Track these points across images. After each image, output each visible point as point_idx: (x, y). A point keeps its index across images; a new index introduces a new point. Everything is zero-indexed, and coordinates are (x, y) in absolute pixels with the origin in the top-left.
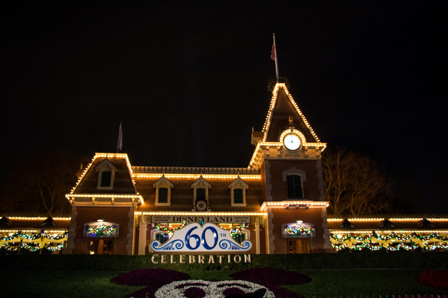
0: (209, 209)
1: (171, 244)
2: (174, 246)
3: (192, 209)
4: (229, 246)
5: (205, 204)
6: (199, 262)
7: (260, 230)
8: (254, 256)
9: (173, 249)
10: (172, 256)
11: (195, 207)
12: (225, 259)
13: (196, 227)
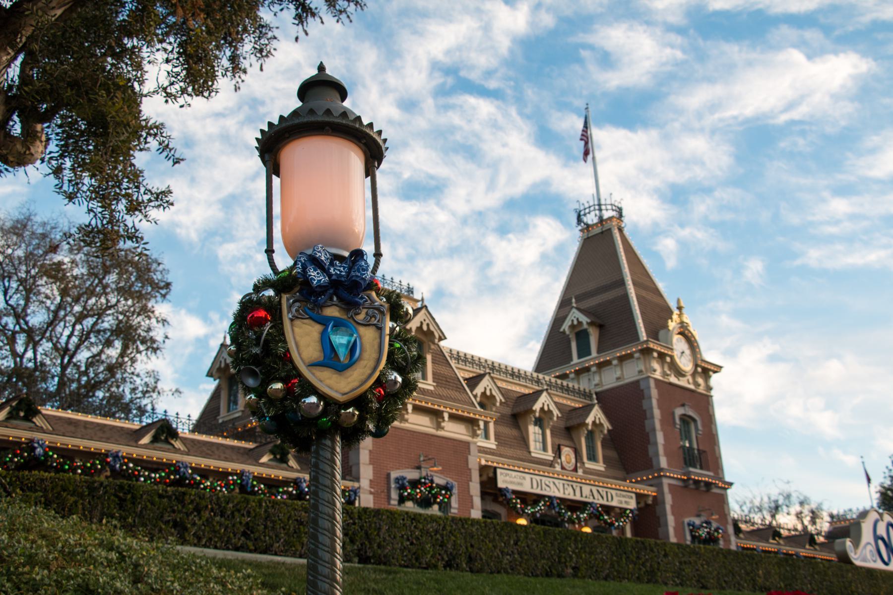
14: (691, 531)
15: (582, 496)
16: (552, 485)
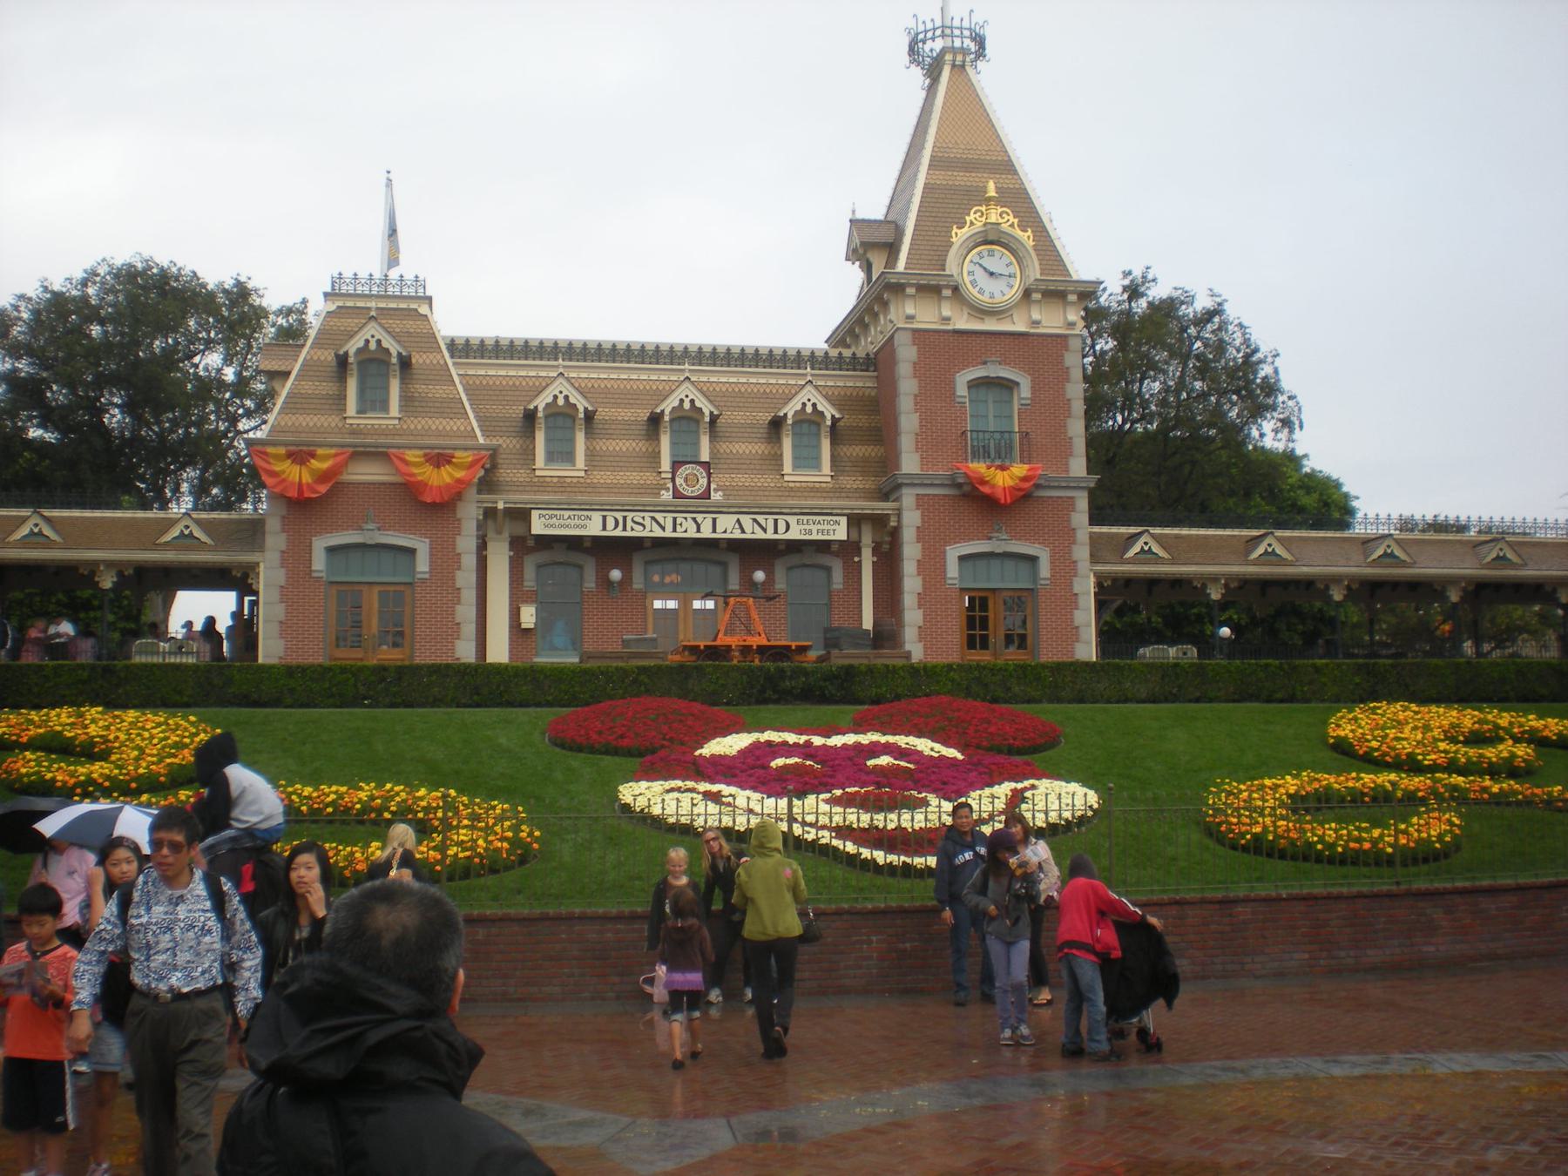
3: (663, 492)
5: (704, 474)
11: (670, 485)
15: (714, 531)
16: (647, 522)
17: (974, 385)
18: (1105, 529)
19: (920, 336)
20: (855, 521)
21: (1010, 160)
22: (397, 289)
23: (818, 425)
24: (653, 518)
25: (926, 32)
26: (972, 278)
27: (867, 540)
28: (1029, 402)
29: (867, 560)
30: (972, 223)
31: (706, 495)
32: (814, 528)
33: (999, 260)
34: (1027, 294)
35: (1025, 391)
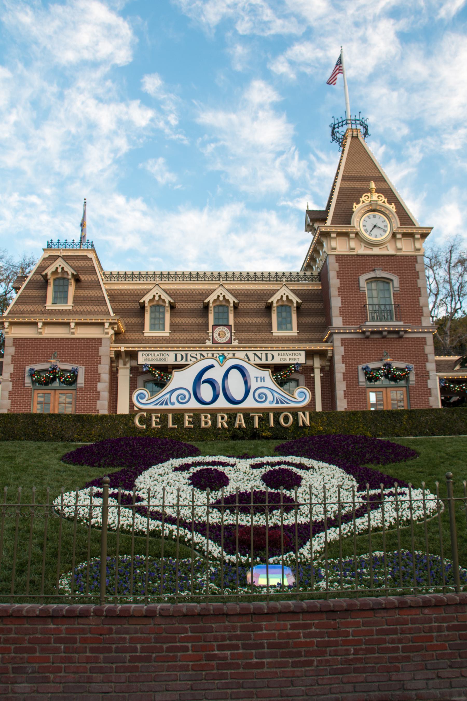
0: (235, 340)
1: (168, 396)
2: (174, 399)
3: (207, 341)
4: (270, 398)
5: (229, 331)
6: (220, 425)
7: (322, 375)
8: (314, 416)
9: (173, 404)
10: (170, 416)
11: (211, 338)
12: (264, 419)
13: (212, 366)
14: (366, 374)
17: (370, 281)
18: (442, 358)
19: (339, 258)
20: (310, 354)
21: (382, 176)
22: (78, 247)
23: (290, 307)
24: (201, 354)
25: (339, 123)
26: (365, 228)
27: (317, 363)
28: (398, 289)
29: (317, 375)
30: (363, 202)
31: (230, 342)
32: (288, 358)
33: (379, 219)
34: (394, 235)
35: (396, 283)
